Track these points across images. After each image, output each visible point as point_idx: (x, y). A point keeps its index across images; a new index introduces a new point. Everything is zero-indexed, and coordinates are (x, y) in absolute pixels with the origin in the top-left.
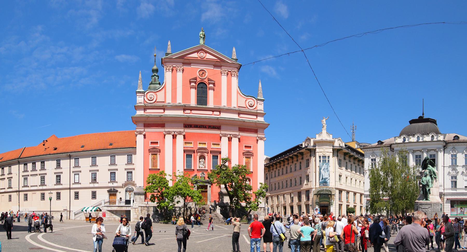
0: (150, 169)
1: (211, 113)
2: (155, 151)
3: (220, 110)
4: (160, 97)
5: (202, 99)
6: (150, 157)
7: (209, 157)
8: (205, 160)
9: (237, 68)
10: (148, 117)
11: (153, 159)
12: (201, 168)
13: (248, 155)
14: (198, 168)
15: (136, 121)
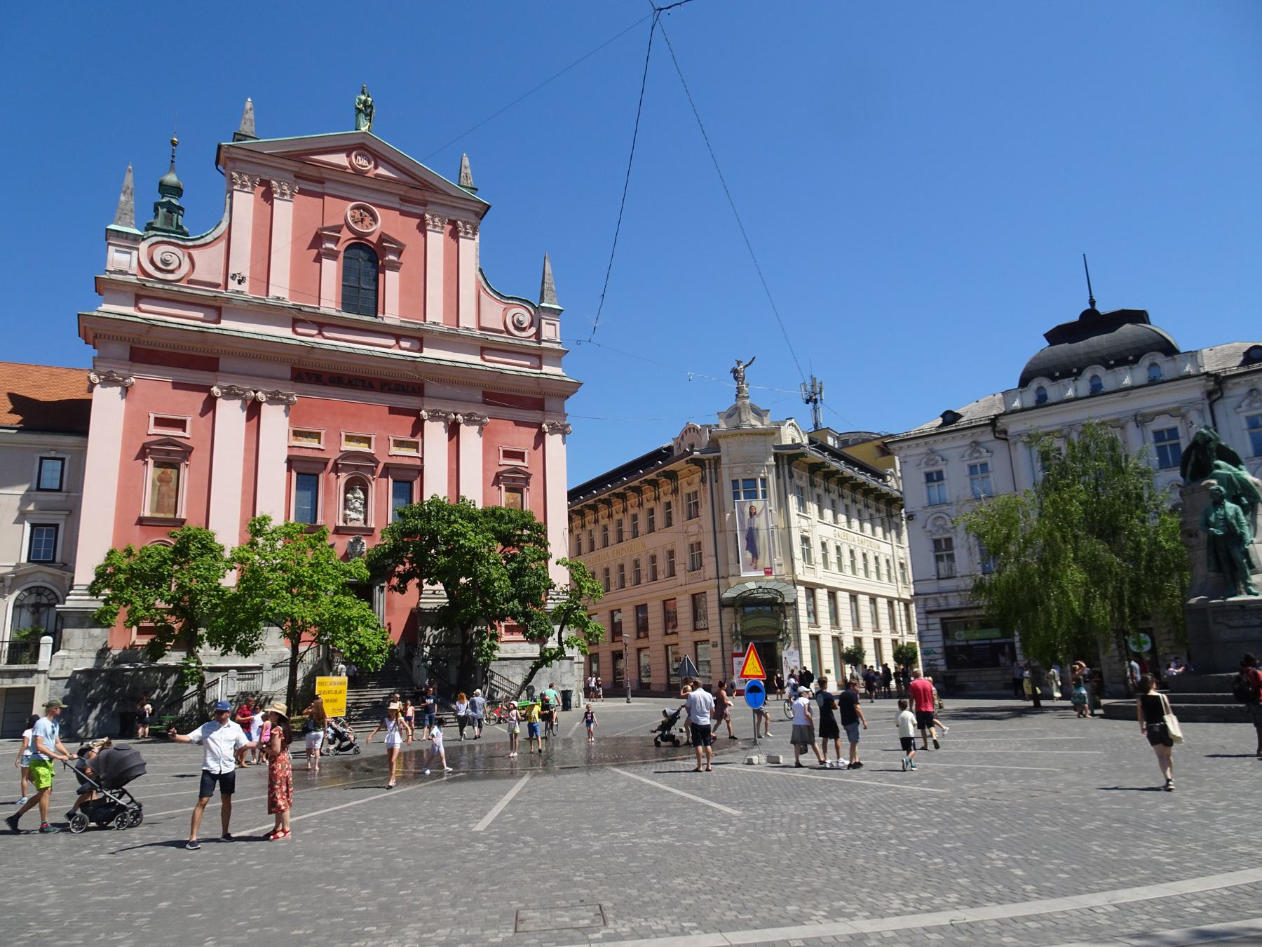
0: (141, 521)
1: (392, 342)
2: (167, 454)
3: (419, 338)
4: (207, 265)
5: (361, 293)
6: (151, 472)
7: (381, 490)
8: (366, 493)
9: (477, 214)
10: (152, 327)
11: (161, 480)
12: (350, 524)
13: (515, 481)
14: (341, 524)
15: (94, 332)
